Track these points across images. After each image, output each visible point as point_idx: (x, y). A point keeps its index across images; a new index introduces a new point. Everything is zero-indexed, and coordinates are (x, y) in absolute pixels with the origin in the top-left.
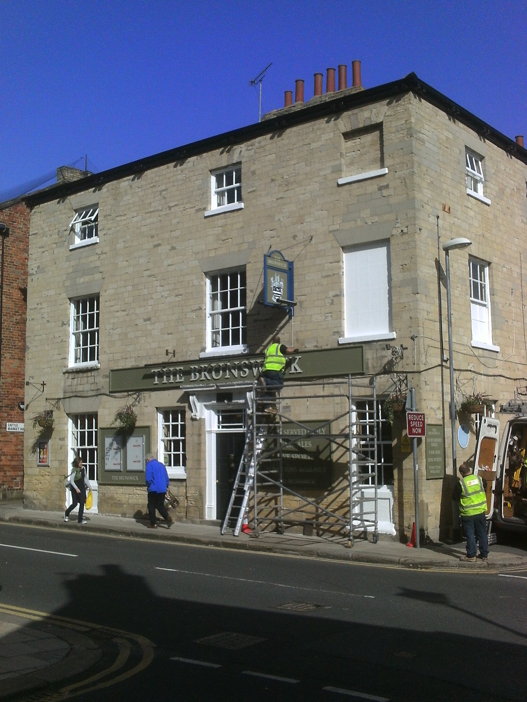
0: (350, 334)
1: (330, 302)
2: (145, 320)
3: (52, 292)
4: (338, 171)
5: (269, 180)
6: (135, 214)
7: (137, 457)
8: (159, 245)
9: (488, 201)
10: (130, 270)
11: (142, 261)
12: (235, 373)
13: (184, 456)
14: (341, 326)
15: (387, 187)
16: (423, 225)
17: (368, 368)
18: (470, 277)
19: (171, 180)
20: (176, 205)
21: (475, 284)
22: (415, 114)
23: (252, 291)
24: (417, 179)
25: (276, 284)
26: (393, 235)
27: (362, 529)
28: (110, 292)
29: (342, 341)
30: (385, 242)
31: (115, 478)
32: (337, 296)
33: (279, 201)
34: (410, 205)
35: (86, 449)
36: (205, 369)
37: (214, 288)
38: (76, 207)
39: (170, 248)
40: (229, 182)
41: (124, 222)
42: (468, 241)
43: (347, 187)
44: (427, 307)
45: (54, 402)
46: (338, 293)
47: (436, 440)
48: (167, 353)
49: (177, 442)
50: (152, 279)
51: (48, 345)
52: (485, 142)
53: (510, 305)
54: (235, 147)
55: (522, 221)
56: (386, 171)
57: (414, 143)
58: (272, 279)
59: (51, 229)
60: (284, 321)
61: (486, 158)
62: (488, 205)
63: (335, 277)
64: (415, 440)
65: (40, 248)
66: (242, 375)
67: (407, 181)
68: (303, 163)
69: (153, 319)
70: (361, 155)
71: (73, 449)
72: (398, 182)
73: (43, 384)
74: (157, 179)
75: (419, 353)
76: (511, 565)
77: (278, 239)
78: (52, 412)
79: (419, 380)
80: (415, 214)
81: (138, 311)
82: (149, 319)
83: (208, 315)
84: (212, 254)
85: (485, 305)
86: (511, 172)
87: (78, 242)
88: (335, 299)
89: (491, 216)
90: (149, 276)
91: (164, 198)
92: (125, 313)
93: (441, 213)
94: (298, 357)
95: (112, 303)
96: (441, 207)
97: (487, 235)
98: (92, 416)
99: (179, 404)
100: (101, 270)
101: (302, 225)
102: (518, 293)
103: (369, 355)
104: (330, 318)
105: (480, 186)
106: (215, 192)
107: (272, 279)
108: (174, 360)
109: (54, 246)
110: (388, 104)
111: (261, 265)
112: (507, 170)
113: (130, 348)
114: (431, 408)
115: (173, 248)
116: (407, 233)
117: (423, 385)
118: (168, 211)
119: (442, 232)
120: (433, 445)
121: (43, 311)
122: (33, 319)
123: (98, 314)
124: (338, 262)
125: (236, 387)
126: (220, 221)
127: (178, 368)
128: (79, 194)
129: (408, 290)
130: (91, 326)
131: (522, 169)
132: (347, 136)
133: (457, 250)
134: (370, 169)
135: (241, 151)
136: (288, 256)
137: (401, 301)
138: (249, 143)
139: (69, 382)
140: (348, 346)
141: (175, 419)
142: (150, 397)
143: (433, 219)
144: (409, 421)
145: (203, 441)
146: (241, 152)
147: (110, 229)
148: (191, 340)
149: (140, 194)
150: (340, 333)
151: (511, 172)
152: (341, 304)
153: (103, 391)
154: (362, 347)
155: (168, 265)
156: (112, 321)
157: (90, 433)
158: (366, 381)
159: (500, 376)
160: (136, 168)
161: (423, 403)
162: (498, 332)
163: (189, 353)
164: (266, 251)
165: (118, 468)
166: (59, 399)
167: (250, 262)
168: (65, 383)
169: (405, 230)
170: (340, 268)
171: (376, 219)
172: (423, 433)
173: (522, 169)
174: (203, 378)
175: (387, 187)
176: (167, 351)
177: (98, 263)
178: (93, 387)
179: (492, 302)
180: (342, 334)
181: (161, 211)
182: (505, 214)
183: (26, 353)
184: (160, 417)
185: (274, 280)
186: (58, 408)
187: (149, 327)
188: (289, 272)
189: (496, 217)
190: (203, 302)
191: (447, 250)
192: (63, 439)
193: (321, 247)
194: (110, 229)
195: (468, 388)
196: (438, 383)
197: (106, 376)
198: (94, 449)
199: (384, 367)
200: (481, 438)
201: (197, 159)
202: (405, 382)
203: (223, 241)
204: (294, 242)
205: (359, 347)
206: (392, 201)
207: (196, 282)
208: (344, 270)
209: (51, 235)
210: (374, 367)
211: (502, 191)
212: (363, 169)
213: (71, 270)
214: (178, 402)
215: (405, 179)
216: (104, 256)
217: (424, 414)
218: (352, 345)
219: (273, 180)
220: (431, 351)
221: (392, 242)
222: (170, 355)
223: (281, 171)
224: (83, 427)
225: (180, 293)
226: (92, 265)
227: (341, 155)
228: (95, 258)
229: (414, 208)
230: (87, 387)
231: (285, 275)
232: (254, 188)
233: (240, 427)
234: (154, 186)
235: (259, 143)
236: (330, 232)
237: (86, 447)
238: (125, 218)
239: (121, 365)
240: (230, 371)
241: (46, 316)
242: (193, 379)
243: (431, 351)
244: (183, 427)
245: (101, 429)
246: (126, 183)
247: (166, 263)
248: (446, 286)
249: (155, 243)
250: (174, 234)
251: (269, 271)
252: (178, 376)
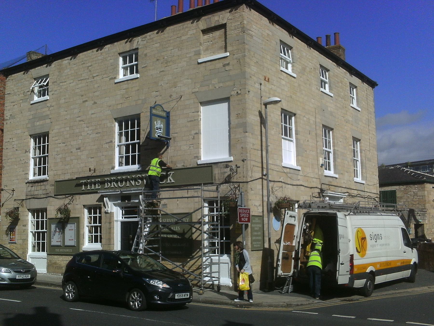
0: (205, 158)
1: (192, 137)
2: (77, 149)
3: (19, 131)
4: (198, 54)
5: (155, 60)
6: (72, 81)
7: (71, 237)
8: (86, 101)
9: (295, 75)
10: (68, 117)
11: (76, 111)
12: (133, 183)
13: (101, 236)
14: (199, 153)
15: (228, 64)
16: (251, 89)
17: (215, 180)
18: (282, 122)
19: (94, 59)
20: (98, 75)
21: (286, 127)
22: (247, 19)
23: (144, 130)
24: (247, 60)
25: (158, 126)
26: (231, 95)
27: (211, 283)
28: (55, 131)
29: (199, 162)
30: (227, 99)
31: (57, 250)
32: (196, 133)
33: (161, 73)
34: (243, 75)
35: (40, 232)
36: (114, 181)
37: (121, 129)
38: (35, 76)
39: (93, 103)
40: (131, 61)
41: (65, 87)
42: (278, 99)
43: (204, 64)
44: (253, 141)
45: (19, 202)
46: (198, 132)
47: (258, 225)
48: (90, 170)
49: (96, 228)
50: (81, 122)
51: (17, 165)
52: (293, 38)
53: (308, 141)
54: (134, 39)
55: (317, 89)
56: (228, 54)
57: (246, 36)
58: (155, 122)
59: (19, 90)
60: (164, 150)
61: (294, 48)
62: (295, 78)
63: (195, 122)
64: (244, 225)
65: (12, 103)
66: (137, 184)
67: (241, 61)
68: (177, 49)
69: (82, 149)
70: (213, 44)
71: (32, 232)
72: (235, 61)
73: (13, 190)
74: (86, 59)
75: (247, 170)
76: (302, 305)
77: (161, 98)
78: (18, 208)
79: (247, 187)
80: (245, 82)
81: (72, 143)
82: (79, 148)
83: (116, 146)
84: (119, 107)
85: (292, 141)
86: (310, 57)
87: (36, 99)
88: (196, 136)
89: (296, 85)
90: (80, 121)
91: (90, 71)
92: (64, 145)
93: (263, 82)
94: (172, 173)
95: (57, 138)
96: (263, 78)
97: (294, 96)
98: (43, 211)
99: (98, 203)
100: (50, 117)
101: (176, 88)
102: (314, 134)
103: (216, 171)
104: (192, 148)
105: (290, 66)
106: (122, 68)
107: (155, 122)
108: (95, 174)
109: (21, 101)
110: (230, 12)
111: (149, 114)
112: (307, 56)
114: (255, 205)
115: (95, 103)
116: (240, 94)
117: (249, 190)
118: (93, 80)
119: (263, 94)
120: (256, 229)
121: (13, 143)
122: (7, 149)
123: (48, 145)
124: (198, 112)
125: (133, 192)
126: (125, 86)
127: (97, 180)
128: (37, 68)
129: (241, 130)
130: (44, 153)
131: (317, 56)
132: (205, 32)
133: (272, 105)
134: (218, 53)
135: (138, 41)
136: (166, 107)
137: (236, 137)
138: (144, 36)
139: (29, 189)
140: (203, 165)
141: (95, 213)
142: (79, 198)
143: (257, 86)
144: (240, 213)
145: (112, 227)
146: (138, 42)
147: (56, 91)
148: (105, 162)
149: (75, 68)
150: (198, 158)
151: (310, 57)
152: (199, 139)
153: (50, 195)
154: (212, 166)
155: (92, 114)
156: (56, 150)
157: (42, 222)
158: (214, 188)
159: (301, 185)
160: (73, 52)
161: (250, 202)
162: (300, 158)
163: (104, 170)
164: (152, 105)
165: (59, 244)
166: (23, 200)
167: (143, 112)
168: (27, 189)
169: (239, 92)
170: (199, 116)
171: (221, 85)
172: (249, 221)
173: (317, 56)
174: (112, 186)
175: (228, 64)
176: (90, 169)
177: (48, 113)
178: (44, 192)
179: (297, 139)
180: (200, 158)
181: (88, 79)
182: (305, 84)
184: (86, 211)
185: (157, 123)
186: (22, 206)
187: (79, 153)
188: (167, 118)
189: (299, 85)
190: (113, 137)
191: (266, 105)
192: (25, 225)
193: (187, 102)
194: (56, 91)
195: (280, 192)
196: (259, 189)
197: (53, 185)
198: (45, 232)
199: (226, 179)
200: (285, 224)
201: (111, 46)
202: (238, 188)
203: (126, 98)
204: (171, 100)
205: (210, 166)
206: (231, 73)
207: (109, 125)
208: (202, 117)
209: (19, 95)
210: (219, 179)
211: (304, 69)
212: (214, 53)
213: (31, 117)
214: (97, 202)
215: (239, 59)
216: (52, 108)
217: (249, 209)
218: (206, 165)
219: (158, 60)
220: (255, 169)
221: (231, 99)
222: (92, 172)
223: (163, 54)
224: (38, 218)
225: (99, 132)
226: (44, 114)
227: (201, 44)
228: (46, 109)
229: (245, 78)
230: (40, 192)
231: (164, 120)
232: (146, 65)
233: (136, 217)
234: (84, 63)
235: (150, 36)
236: (193, 93)
237: (40, 230)
238: (65, 84)
239: (62, 178)
240: (129, 181)
241: (15, 146)
242: (106, 187)
243: (255, 169)
244: (100, 218)
245: (49, 219)
246: (67, 62)
247: (90, 112)
248: (265, 128)
249: (84, 100)
250: (96, 94)
251: (153, 117)
252: (97, 185)
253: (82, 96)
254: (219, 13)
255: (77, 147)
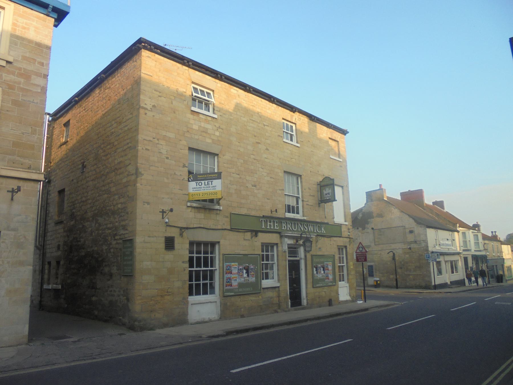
6: (243, 115)
90: (255, 159)
92: (239, 176)
113: (243, 201)
115: (267, 149)
141: (267, 251)
183: (138, 179)
186: (181, 235)
187: (256, 191)
197: (227, 217)
233: (296, 257)
241: (164, 152)
253: (255, 136)
254: (338, 133)
255: (253, 184)
